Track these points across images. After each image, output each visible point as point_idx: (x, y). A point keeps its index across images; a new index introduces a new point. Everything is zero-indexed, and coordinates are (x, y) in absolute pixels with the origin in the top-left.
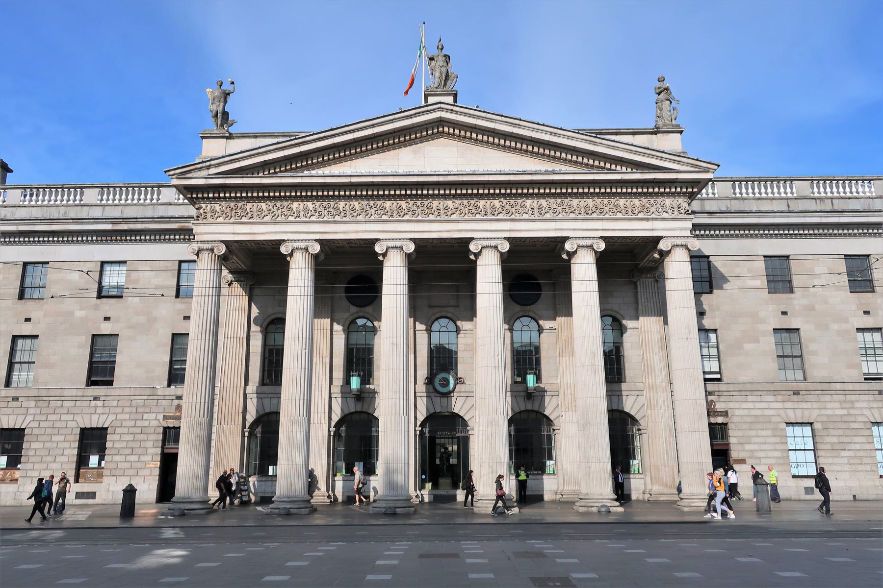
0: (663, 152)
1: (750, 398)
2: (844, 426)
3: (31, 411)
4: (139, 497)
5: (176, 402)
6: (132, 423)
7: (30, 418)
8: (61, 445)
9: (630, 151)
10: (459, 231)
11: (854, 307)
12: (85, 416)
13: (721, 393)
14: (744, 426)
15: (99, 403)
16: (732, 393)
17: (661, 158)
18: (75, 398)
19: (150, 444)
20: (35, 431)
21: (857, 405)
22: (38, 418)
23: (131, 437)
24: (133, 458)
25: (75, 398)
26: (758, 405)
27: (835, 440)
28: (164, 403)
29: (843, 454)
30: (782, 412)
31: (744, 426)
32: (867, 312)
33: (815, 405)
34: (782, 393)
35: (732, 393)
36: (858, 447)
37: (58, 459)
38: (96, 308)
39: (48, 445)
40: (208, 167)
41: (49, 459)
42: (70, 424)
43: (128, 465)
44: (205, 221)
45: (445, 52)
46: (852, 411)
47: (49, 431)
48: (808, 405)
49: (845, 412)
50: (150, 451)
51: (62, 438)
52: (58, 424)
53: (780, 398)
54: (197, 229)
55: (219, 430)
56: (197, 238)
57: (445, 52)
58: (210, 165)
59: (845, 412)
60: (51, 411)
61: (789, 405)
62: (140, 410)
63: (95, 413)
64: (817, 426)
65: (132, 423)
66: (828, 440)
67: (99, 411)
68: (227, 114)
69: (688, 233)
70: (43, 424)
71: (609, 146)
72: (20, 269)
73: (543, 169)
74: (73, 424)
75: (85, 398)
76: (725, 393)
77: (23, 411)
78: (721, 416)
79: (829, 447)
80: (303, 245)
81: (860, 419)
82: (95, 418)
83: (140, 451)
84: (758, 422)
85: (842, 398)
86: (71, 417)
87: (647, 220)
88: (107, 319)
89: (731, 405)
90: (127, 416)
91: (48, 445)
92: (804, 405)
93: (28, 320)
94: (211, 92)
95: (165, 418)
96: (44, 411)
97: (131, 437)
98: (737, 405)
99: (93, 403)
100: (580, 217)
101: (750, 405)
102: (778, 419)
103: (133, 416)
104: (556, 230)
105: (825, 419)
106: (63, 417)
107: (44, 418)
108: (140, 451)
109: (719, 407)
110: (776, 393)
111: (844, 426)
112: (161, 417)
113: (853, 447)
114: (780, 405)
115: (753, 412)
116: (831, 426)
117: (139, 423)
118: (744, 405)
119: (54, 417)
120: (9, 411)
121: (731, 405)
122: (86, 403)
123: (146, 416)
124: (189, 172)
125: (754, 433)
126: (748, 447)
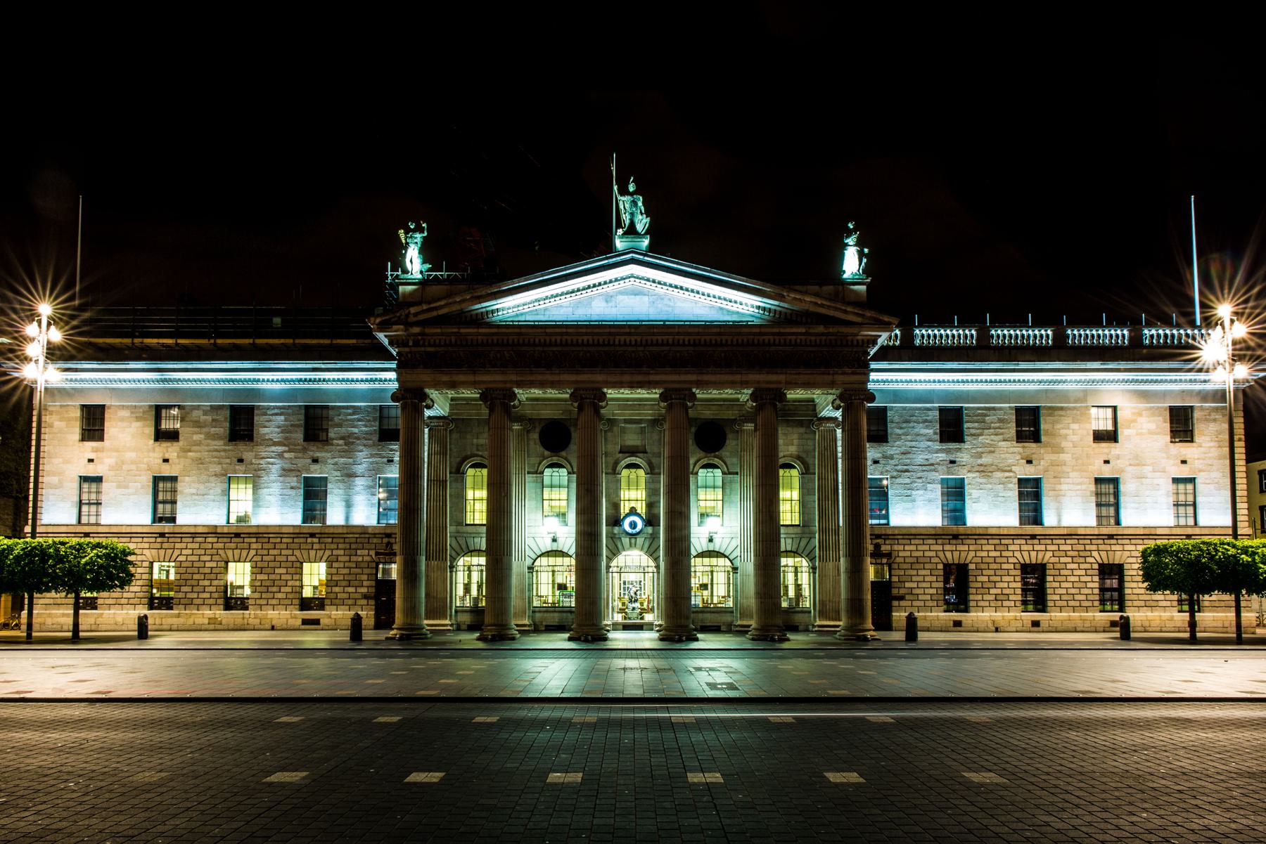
2: (995, 566)
3: (254, 546)
4: (364, 622)
5: (385, 540)
6: (347, 558)
8: (283, 577)
11: (1018, 457)
14: (905, 566)
15: (316, 540)
19: (365, 577)
21: (1011, 548)
22: (260, 552)
23: (346, 571)
24: (351, 590)
26: (920, 548)
27: (986, 579)
28: (375, 541)
29: (992, 591)
30: (941, 554)
31: (905, 566)
32: (1029, 462)
33: (972, 548)
36: (1006, 585)
37: (283, 589)
39: (272, 577)
41: (274, 589)
42: (290, 558)
43: (346, 596)
46: (1004, 554)
47: (271, 564)
48: (966, 548)
49: (998, 554)
50: (365, 583)
51: (284, 571)
52: (278, 558)
53: (940, 541)
55: (427, 565)
60: (271, 546)
61: (947, 547)
62: (353, 546)
65: (347, 558)
66: (980, 579)
70: (265, 558)
77: (246, 545)
79: (979, 585)
81: (1011, 560)
83: (357, 583)
84: (917, 562)
86: (290, 552)
89: (896, 547)
90: (342, 552)
91: (272, 577)
92: (960, 548)
93: (240, 461)
95: (377, 554)
96: (266, 546)
97: (346, 571)
98: (901, 548)
99: (309, 540)
101: (913, 548)
102: (937, 560)
103: (347, 552)
105: (979, 560)
106: (284, 552)
107: (265, 552)
108: (357, 583)
109: (885, 548)
111: (995, 566)
112: (373, 553)
113: (1001, 585)
114: (940, 548)
116: (983, 566)
117: (354, 559)
119: (275, 552)
120: (233, 545)
121: (896, 547)
122: (302, 540)
123: (359, 552)
125: (914, 572)
126: (907, 585)
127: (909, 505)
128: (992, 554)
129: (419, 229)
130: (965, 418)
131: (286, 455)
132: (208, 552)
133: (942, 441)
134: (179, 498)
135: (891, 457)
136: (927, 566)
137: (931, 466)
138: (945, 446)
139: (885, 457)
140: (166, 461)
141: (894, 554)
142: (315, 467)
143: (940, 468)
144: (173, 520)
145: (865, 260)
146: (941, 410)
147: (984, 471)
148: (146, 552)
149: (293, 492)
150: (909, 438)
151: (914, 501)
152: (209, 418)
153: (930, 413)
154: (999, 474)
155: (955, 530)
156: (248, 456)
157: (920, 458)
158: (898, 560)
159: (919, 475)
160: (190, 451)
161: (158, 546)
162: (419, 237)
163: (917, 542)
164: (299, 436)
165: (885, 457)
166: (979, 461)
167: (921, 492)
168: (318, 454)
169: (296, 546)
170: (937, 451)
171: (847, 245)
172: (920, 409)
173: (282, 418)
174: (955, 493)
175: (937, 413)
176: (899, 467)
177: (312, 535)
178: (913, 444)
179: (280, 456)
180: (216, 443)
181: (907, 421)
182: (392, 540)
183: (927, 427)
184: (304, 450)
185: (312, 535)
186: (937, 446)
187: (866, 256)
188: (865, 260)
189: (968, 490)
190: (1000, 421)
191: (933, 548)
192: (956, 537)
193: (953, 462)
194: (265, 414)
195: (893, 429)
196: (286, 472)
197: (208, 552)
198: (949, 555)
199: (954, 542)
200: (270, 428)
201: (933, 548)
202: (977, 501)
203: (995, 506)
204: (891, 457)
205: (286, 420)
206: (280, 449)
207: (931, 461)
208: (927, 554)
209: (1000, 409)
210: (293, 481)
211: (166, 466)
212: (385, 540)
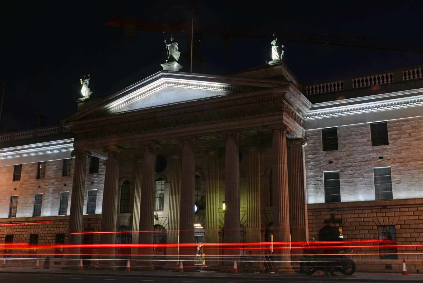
1: (356, 212)
2: (414, 226)
5: (88, 222)
7: (40, 230)
12: (58, 228)
13: (338, 210)
15: (62, 223)
16: (344, 209)
18: (54, 221)
20: (42, 235)
25: (54, 221)
27: (408, 235)
30: (375, 219)
33: (397, 214)
34: (376, 208)
35: (344, 209)
47: (46, 235)
49: (416, 217)
53: (374, 211)
59: (416, 217)
61: (379, 214)
63: (61, 227)
64: (398, 227)
67: (62, 226)
70: (44, 232)
72: (36, 166)
74: (53, 232)
75: (57, 221)
76: (340, 209)
78: (338, 222)
82: (61, 229)
85: (416, 209)
92: (388, 214)
93: (39, 187)
98: (348, 216)
102: (372, 223)
107: (44, 229)
110: (371, 208)
111: (414, 226)
114: (375, 215)
115: (358, 220)
116: (405, 226)
118: (352, 216)
122: (58, 223)
127: (353, 188)
128: (412, 218)
129: (87, 78)
130: (389, 129)
131: (55, 183)
132: (25, 230)
133: (372, 146)
134: (18, 206)
135: (340, 159)
136: (366, 228)
137: (367, 162)
138: (375, 148)
139: (336, 159)
140: (15, 189)
141: (343, 222)
142: (65, 188)
143: (372, 162)
144: (15, 216)
145: (283, 52)
146: (372, 125)
147: (403, 162)
148: (5, 231)
149: (56, 201)
150: (351, 145)
151: (356, 185)
152: (31, 169)
153: (364, 128)
154: (414, 163)
155: (385, 202)
156: (42, 185)
157: (359, 157)
158: (346, 224)
159: (358, 168)
160: (23, 184)
161: (9, 228)
162: (87, 81)
163: (359, 212)
164: (60, 174)
165: (336, 159)
166: (400, 156)
167: (360, 179)
168: (67, 182)
169: (55, 226)
170: (370, 152)
171: (272, 45)
172: (357, 126)
173: (55, 166)
174: (384, 181)
175: (369, 128)
176: (346, 164)
177: (61, 221)
178: (354, 149)
179: (53, 184)
180: (32, 180)
181: (350, 135)
182: (91, 222)
183: (363, 137)
184: (62, 180)
185: (61, 221)
186: (371, 148)
187: (283, 49)
188: (283, 52)
189: (393, 175)
190: (413, 127)
191: (369, 215)
192: (384, 207)
193: (381, 158)
194: (50, 165)
195: (341, 141)
196: (55, 191)
197: (25, 230)
198: (381, 220)
199: (384, 210)
200: (50, 172)
201: (369, 215)
202: (399, 182)
203: (413, 185)
204: (340, 159)
205: (56, 167)
206: (53, 181)
207: (366, 159)
208: (365, 220)
209: (412, 120)
210: (56, 195)
211: (15, 192)
212: (88, 222)
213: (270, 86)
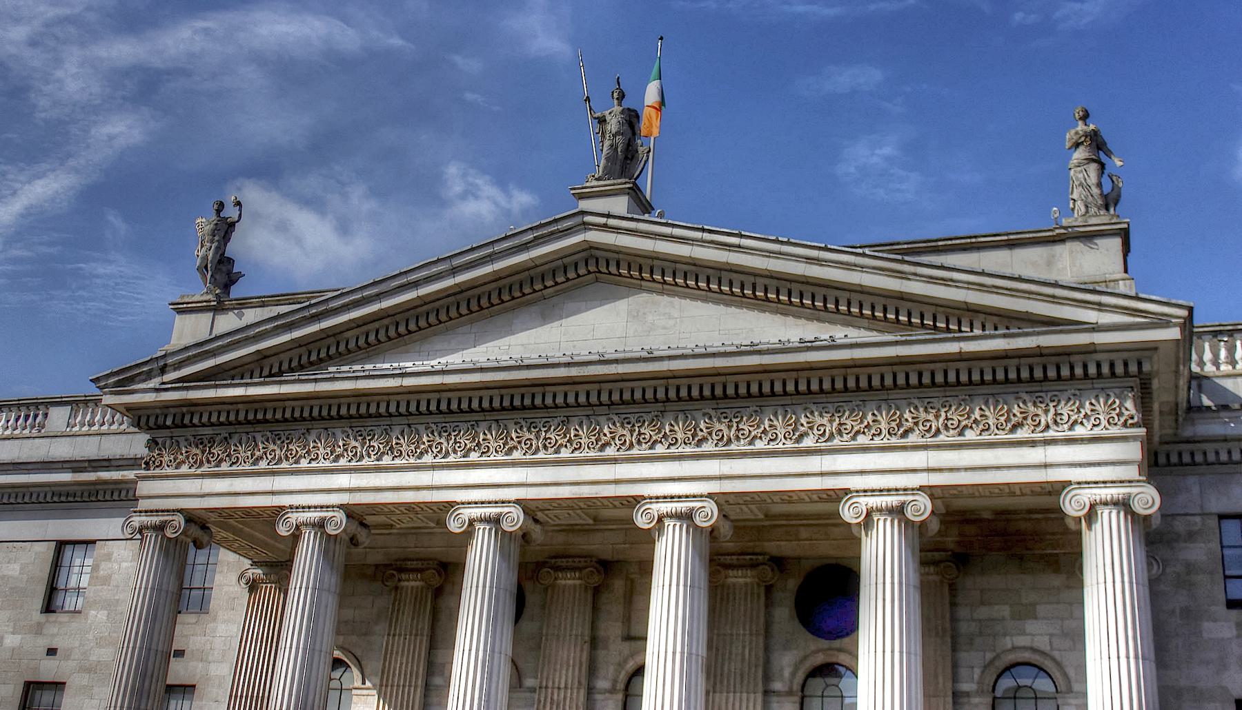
0: (1056, 285)
9: (982, 287)
10: (617, 482)
17: (1054, 299)
38: (38, 630)
40: (163, 370)
44: (158, 471)
45: (627, 103)
54: (144, 488)
56: (143, 505)
57: (627, 103)
58: (165, 365)
68: (230, 261)
69: (1132, 472)
71: (932, 280)
73: (795, 338)
80: (314, 515)
87: (1032, 443)
88: (52, 652)
94: (204, 223)
100: (877, 441)
104: (822, 474)
124: (131, 380)
213: (1091, 316)
